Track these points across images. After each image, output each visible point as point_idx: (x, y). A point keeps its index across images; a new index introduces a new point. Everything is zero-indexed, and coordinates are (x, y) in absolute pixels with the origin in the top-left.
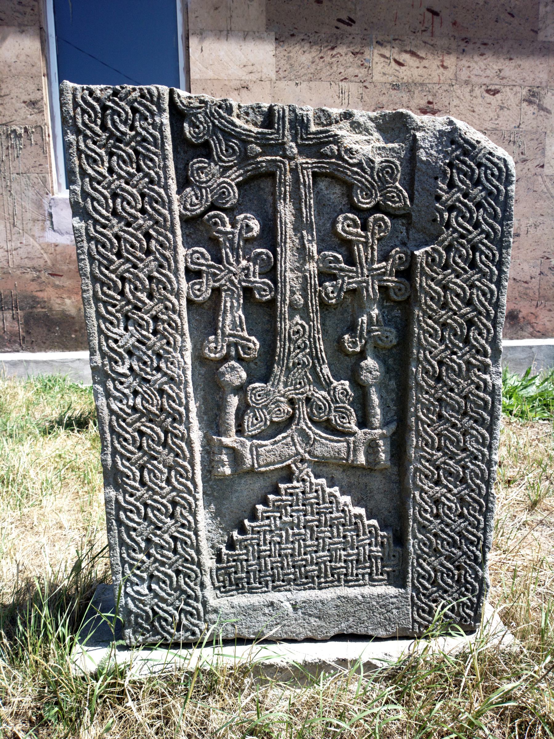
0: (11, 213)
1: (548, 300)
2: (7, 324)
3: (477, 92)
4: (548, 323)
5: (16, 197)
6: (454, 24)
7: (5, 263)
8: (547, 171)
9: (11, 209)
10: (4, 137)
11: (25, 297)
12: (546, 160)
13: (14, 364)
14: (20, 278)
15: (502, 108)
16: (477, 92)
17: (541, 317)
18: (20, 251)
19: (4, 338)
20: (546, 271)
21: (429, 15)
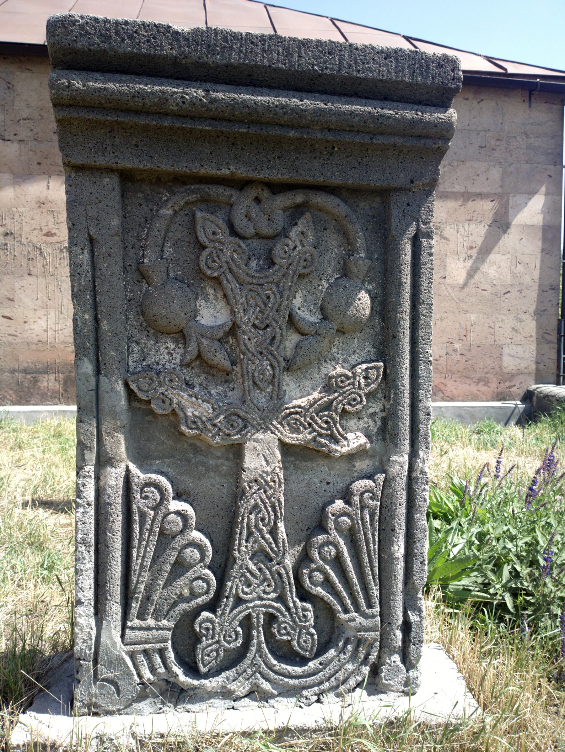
0: (60, 304)
1: (454, 373)
2: (50, 384)
4: (454, 391)
5: (65, 293)
7: (53, 340)
8: (448, 281)
9: (60, 301)
10: (58, 251)
11: (66, 365)
12: (447, 273)
13: (56, 413)
14: (63, 350)
17: (449, 386)
18: (65, 331)
19: (47, 394)
20: (451, 352)
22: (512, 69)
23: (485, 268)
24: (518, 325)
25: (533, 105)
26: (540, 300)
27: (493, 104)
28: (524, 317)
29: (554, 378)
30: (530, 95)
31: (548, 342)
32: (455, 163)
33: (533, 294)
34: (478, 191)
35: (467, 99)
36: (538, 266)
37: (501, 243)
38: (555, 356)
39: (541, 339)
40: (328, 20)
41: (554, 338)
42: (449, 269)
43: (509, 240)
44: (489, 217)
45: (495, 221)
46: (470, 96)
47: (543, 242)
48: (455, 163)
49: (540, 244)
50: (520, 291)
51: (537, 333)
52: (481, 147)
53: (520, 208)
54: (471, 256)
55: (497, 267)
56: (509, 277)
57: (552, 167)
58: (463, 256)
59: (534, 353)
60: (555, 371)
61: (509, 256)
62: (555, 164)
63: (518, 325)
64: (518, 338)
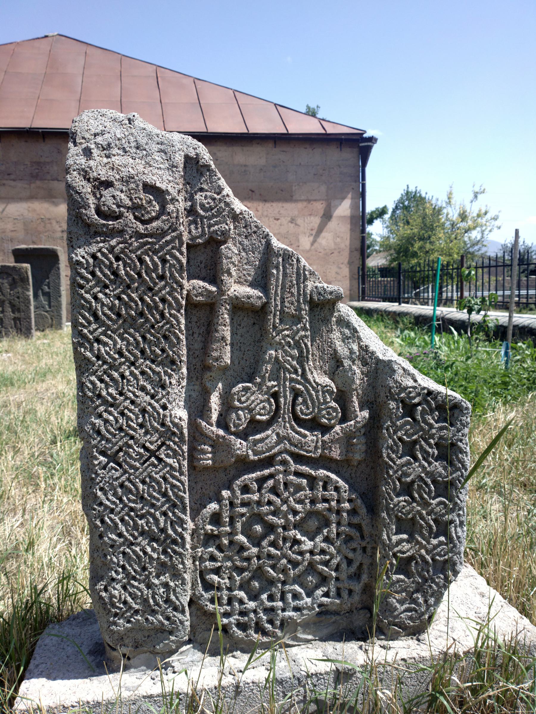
3: (271, 219)
6: (260, 195)
15: (281, 225)
16: (271, 219)
21: (250, 192)
22: (331, 129)
23: (319, 240)
26: (350, 257)
27: (320, 150)
28: (342, 266)
29: (357, 298)
30: (341, 144)
31: (355, 279)
32: (301, 184)
35: (306, 148)
36: (348, 238)
37: (328, 226)
38: (357, 286)
39: (351, 278)
40: (231, 92)
41: (357, 277)
42: (301, 241)
43: (332, 224)
44: (322, 212)
45: (324, 215)
48: (301, 184)
49: (349, 226)
50: (339, 252)
52: (315, 175)
53: (336, 207)
55: (326, 240)
56: (333, 245)
57: (354, 184)
58: (308, 234)
59: (348, 285)
60: (357, 295)
62: (356, 182)
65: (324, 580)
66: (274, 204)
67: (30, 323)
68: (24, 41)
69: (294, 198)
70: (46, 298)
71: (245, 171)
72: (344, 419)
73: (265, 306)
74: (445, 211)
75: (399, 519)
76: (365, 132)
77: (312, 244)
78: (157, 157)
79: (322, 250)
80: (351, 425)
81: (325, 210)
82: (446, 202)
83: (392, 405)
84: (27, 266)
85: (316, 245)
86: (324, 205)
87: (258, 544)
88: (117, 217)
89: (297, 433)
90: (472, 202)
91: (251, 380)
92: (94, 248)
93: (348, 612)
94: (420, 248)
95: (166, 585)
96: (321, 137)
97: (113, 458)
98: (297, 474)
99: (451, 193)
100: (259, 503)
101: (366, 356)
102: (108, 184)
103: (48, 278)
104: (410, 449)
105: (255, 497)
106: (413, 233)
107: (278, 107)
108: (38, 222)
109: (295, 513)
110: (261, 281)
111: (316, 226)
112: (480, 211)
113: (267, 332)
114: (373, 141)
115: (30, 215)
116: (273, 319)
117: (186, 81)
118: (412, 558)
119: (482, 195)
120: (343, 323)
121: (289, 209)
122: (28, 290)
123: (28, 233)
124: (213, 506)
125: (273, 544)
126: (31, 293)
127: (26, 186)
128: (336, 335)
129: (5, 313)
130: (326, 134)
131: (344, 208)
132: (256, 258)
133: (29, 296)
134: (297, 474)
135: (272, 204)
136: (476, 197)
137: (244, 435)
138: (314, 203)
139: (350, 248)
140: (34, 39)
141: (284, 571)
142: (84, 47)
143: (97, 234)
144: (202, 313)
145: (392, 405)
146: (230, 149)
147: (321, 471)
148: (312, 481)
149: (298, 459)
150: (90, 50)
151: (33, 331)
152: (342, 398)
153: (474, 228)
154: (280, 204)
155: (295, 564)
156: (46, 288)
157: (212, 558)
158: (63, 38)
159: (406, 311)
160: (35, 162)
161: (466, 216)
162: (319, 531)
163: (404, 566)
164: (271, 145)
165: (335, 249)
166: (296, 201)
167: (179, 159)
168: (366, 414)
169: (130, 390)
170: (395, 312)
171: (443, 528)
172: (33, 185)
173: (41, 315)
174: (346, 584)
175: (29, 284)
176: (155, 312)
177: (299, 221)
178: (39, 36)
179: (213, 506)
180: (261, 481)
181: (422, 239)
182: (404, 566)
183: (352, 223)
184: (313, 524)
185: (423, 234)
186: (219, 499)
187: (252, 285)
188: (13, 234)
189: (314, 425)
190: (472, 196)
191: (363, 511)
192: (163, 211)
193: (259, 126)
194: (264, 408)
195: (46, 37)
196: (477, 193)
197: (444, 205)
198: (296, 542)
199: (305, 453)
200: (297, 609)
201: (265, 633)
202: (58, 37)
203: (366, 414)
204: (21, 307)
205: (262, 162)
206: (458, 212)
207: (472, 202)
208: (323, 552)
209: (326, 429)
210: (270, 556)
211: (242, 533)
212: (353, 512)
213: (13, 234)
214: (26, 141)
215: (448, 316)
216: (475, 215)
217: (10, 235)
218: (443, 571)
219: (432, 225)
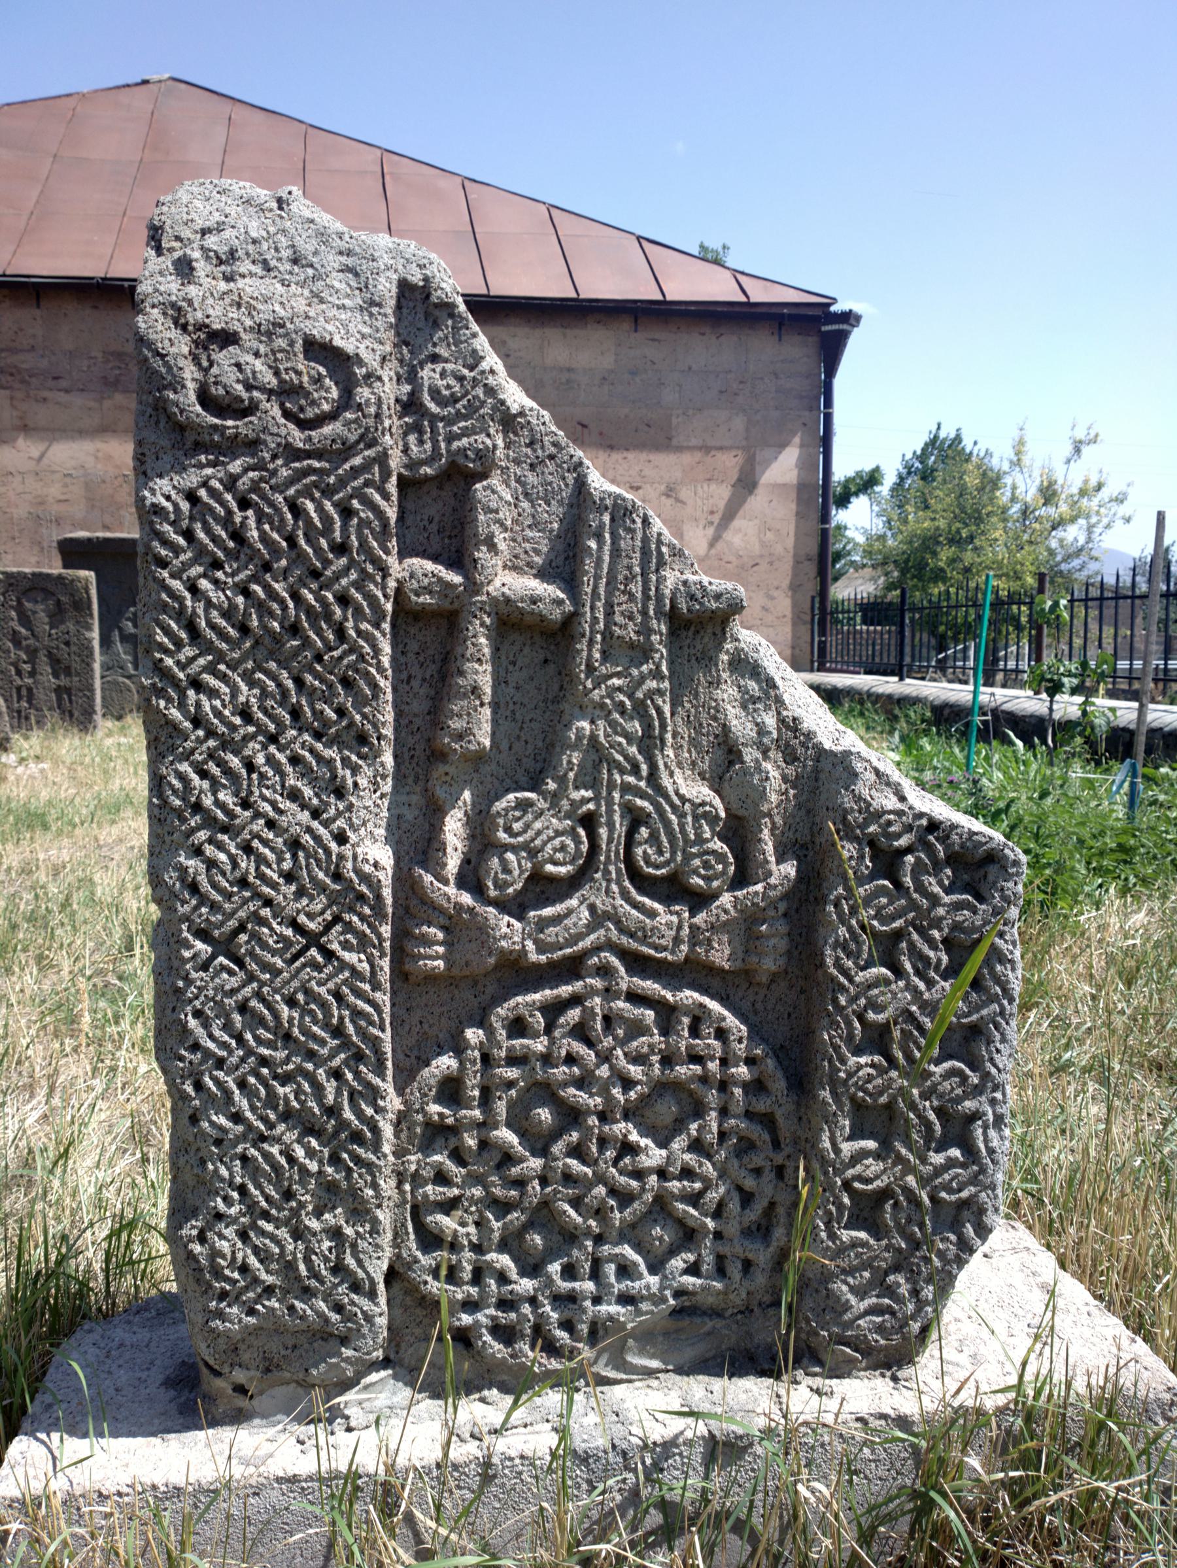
22: (759, 294)
23: (728, 535)
24: (769, 604)
25: (784, 338)
26: (795, 574)
27: (735, 338)
28: (776, 593)
30: (781, 325)
31: (805, 623)
32: (691, 412)
33: (785, 568)
34: (718, 444)
36: (792, 534)
37: (747, 506)
39: (796, 620)
40: (543, 208)
41: (808, 618)
42: (686, 538)
43: (757, 502)
44: (734, 475)
45: (739, 480)
46: (708, 330)
47: (798, 504)
49: (793, 506)
50: (771, 563)
51: (793, 612)
53: (767, 463)
54: (712, 523)
55: (744, 534)
57: (807, 413)
58: (702, 522)
59: (789, 636)
60: (808, 657)
61: (757, 521)
62: (811, 409)
63: (769, 604)
64: (770, 618)
65: (688, 1236)
66: (631, 455)
67: (91, 699)
68: (96, 91)
69: (674, 442)
70: (129, 647)
71: (568, 381)
72: (741, 880)
73: (570, 620)
74: (1008, 480)
75: (858, 1107)
76: (835, 300)
77: (712, 545)
78: (338, 282)
79: (732, 558)
80: (756, 893)
81: (741, 471)
82: (1011, 462)
83: (848, 850)
84: (90, 575)
85: (720, 545)
86: (740, 460)
87: (542, 1151)
88: (246, 411)
89: (636, 905)
90: (1068, 461)
91: (535, 785)
92: (192, 479)
93: (741, 1312)
94: (952, 561)
95: (335, 1233)
96: (737, 309)
97: (225, 946)
98: (634, 997)
99: (1021, 442)
100: (547, 1059)
101: (792, 739)
102: (227, 338)
103: (134, 604)
104: (888, 950)
105: (539, 1045)
106: (938, 528)
107: (645, 243)
108: (116, 483)
109: (627, 1083)
110: (564, 566)
111: (722, 505)
112: (1086, 482)
113: (573, 679)
114: (852, 321)
115: (99, 466)
116: (588, 651)
117: (444, 183)
118: (885, 1194)
119: (1093, 446)
120: (745, 666)
121: (665, 466)
122: (89, 628)
123: (93, 506)
124: (446, 1063)
125: (577, 1151)
126: (95, 635)
127: (92, 404)
128: (728, 694)
129: (39, 677)
130: (749, 304)
131: (784, 467)
132: (552, 515)
133: (90, 641)
134: (634, 997)
135: (626, 454)
136: (1078, 451)
137: (516, 907)
138: (719, 454)
139: (795, 555)
140: (118, 87)
141: (600, 1212)
142: (226, 108)
143: (199, 447)
144: (431, 632)
145: (848, 850)
146: (538, 332)
147: (688, 993)
148: (667, 1014)
149: (637, 963)
150: (239, 113)
151: (98, 718)
152: (738, 831)
153: (1073, 520)
154: (644, 456)
155: (625, 1198)
156: (129, 627)
157: (441, 1178)
158: (183, 86)
159: (914, 694)
160: (112, 354)
161: (1055, 493)
162: (679, 1126)
163: (868, 1210)
164: (626, 325)
165: (761, 556)
166: (679, 449)
167: (386, 288)
168: (790, 869)
169: (266, 798)
170: (890, 697)
171: (958, 1130)
172: (107, 403)
173: (117, 683)
174: (737, 1248)
175: (91, 615)
176: (324, 626)
177: (685, 493)
178: (130, 81)
179: (446, 1063)
180: (553, 1010)
181: (955, 540)
182: (868, 1210)
183: (800, 501)
184: (667, 1109)
185: (958, 531)
186: (459, 1048)
187: (542, 574)
188: (62, 508)
189: (673, 889)
190: (1068, 449)
191: (779, 1085)
192: (347, 400)
193: (603, 283)
194: (563, 848)
195: (145, 82)
196: (1080, 442)
197: (1006, 467)
198: (628, 1149)
199: (652, 952)
200: (626, 1299)
201: (551, 1349)
202: (170, 83)
203: (790, 869)
204: (74, 665)
205: (607, 362)
206: (1038, 483)
207: (1068, 461)
208: (687, 1173)
209: (699, 900)
210: (568, 1178)
211: (509, 1126)
212: (756, 1087)
213: (62, 508)
214: (96, 307)
215: (1005, 707)
216: (1075, 490)
217: (55, 509)
218: (956, 1226)
219: (978, 511)
